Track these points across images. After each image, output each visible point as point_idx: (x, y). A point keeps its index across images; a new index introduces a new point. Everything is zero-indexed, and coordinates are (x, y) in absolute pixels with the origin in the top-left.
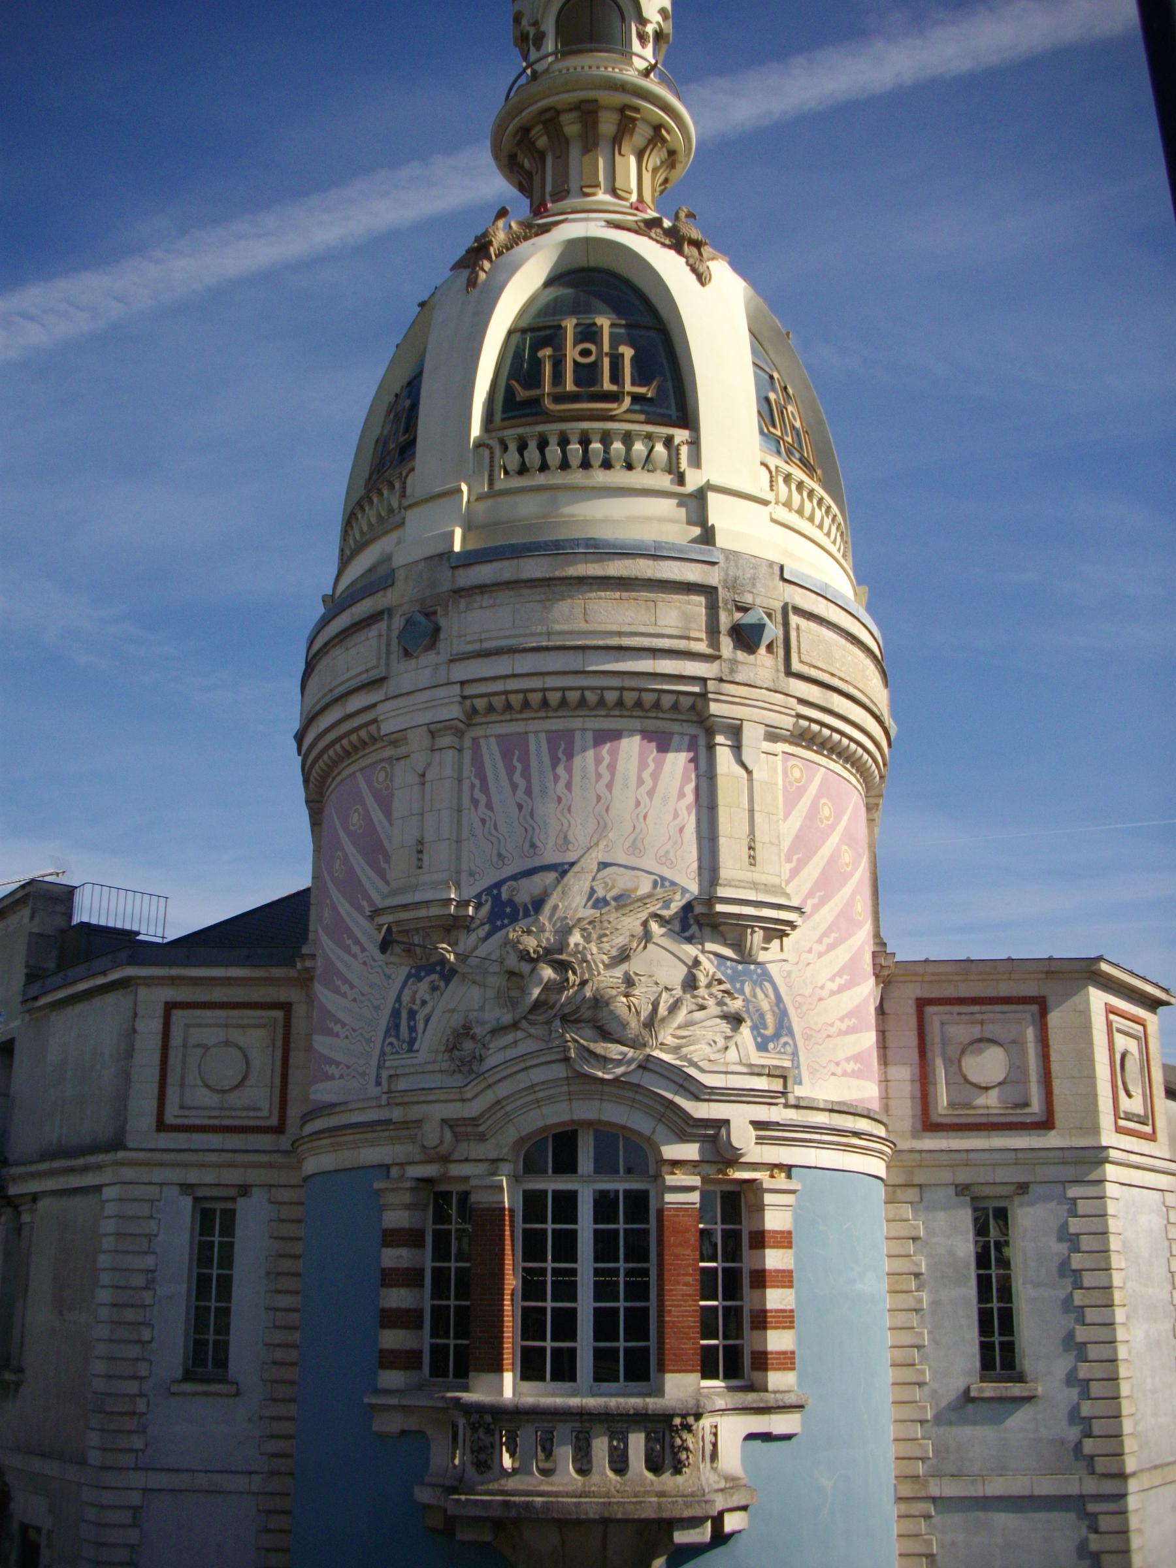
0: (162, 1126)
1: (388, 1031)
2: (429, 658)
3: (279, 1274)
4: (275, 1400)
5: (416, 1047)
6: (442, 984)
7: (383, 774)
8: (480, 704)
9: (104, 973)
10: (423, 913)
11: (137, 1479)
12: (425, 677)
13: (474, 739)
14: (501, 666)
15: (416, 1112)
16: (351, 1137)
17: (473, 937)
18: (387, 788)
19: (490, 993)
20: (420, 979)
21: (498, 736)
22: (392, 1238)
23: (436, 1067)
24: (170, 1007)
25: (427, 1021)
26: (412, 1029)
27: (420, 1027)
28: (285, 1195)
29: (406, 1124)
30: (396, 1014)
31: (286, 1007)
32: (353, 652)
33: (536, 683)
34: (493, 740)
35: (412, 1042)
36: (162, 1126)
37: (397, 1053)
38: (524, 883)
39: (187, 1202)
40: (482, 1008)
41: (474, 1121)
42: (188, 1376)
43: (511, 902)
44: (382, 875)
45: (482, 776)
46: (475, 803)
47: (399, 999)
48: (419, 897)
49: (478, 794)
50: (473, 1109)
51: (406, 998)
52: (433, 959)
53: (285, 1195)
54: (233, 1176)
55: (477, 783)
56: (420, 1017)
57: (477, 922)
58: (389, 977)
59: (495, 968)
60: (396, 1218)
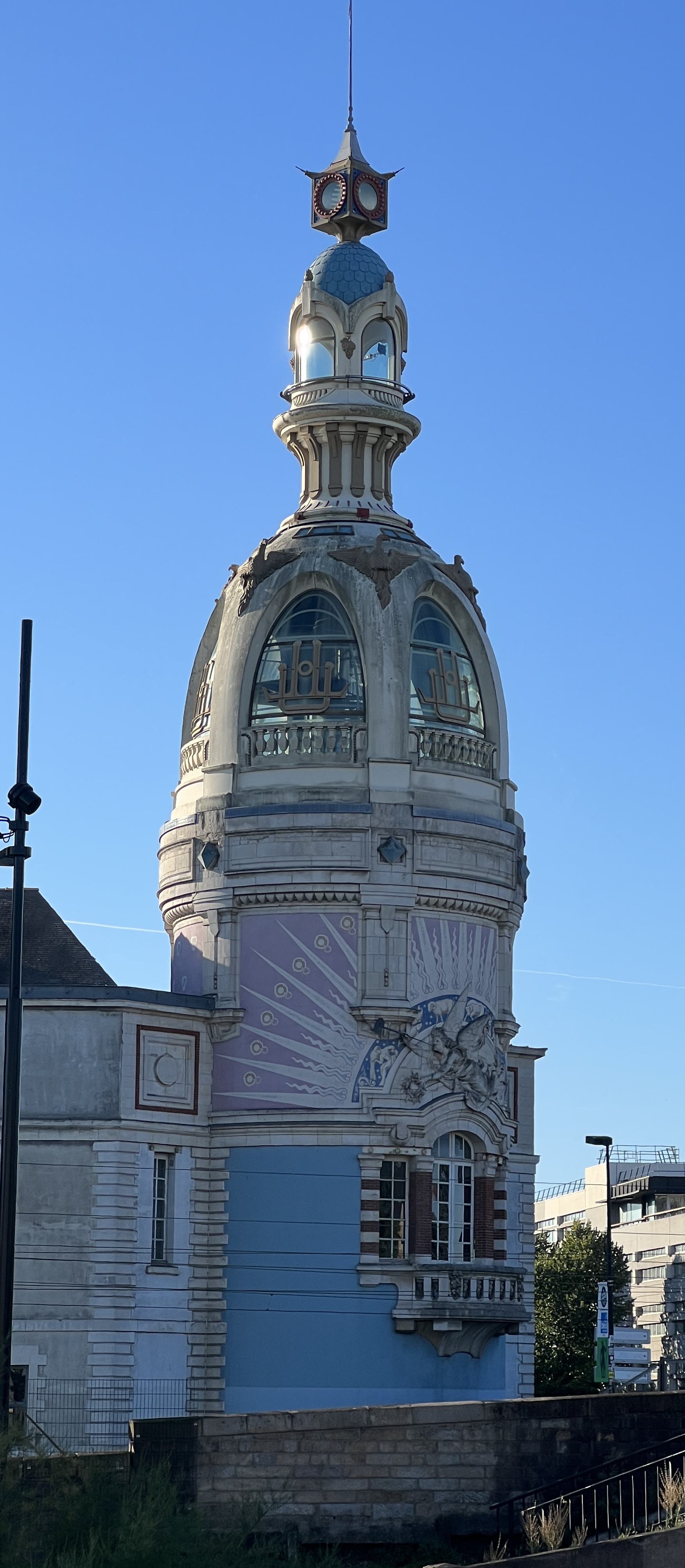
0: (138, 1106)
1: (360, 1073)
2: (397, 867)
3: (196, 1201)
4: (195, 1278)
5: (381, 1084)
6: (396, 1052)
7: (347, 923)
8: (424, 900)
9: (95, 1000)
10: (395, 1013)
11: (134, 1326)
12: (397, 878)
13: (413, 917)
14: (439, 882)
15: (392, 1120)
16: (340, 1129)
17: (414, 1029)
18: (352, 931)
19: (424, 1061)
20: (383, 1047)
21: (425, 918)
22: (366, 1184)
23: (399, 1097)
24: (140, 1027)
25: (388, 1071)
26: (378, 1074)
27: (383, 1075)
28: (198, 1153)
29: (383, 1126)
30: (366, 1064)
31: (196, 1034)
32: (336, 845)
33: (453, 895)
34: (422, 920)
35: (378, 1082)
36: (138, 1106)
37: (368, 1085)
38: (438, 1002)
39: (151, 1154)
40: (420, 1068)
41: (422, 1127)
42: (154, 1264)
43: (432, 1013)
44: (351, 983)
45: (417, 939)
46: (414, 954)
47: (368, 1055)
48: (389, 1004)
49: (415, 949)
50: (423, 1122)
51: (373, 1055)
52: (391, 1038)
53: (198, 1153)
54: (175, 1140)
55: (414, 943)
56: (383, 1068)
57: (416, 1022)
58: (360, 1043)
59: (426, 1047)
60: (373, 1174)
